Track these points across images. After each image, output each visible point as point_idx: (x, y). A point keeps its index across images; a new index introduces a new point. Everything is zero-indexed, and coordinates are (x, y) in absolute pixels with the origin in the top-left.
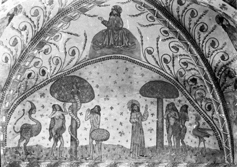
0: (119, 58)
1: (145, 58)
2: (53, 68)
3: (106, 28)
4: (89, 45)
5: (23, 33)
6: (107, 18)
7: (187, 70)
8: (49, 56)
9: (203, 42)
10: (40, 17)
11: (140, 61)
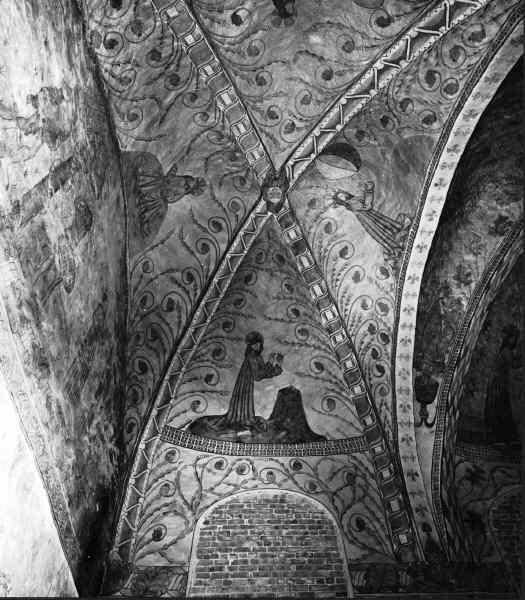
3: (165, 173)
7: (147, 345)
9: (211, 338)
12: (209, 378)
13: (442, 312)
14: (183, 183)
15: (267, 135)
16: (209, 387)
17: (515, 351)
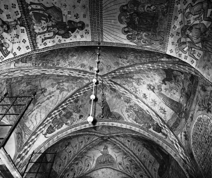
0: (107, 168)
1: (119, 167)
2: (79, 172)
3: (102, 154)
4: (95, 162)
5: (70, 154)
6: (102, 150)
8: (78, 166)
9: (141, 156)
10: (77, 148)
11: (116, 169)
12: (150, 162)
13: (137, 110)
14: (105, 150)
15: (93, 139)
16: (153, 163)
17: (156, 88)
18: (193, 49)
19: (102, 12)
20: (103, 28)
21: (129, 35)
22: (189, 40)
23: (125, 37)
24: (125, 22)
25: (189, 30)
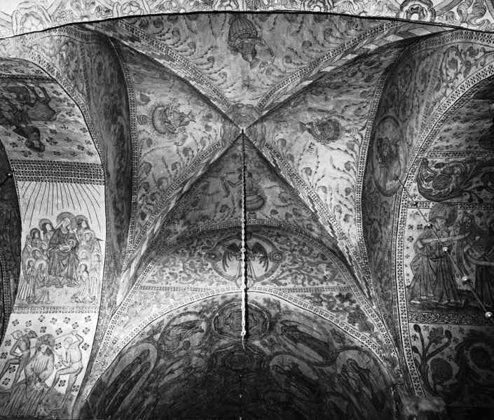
18: (17, 366)
19: (71, 182)
20: (44, 183)
21: (39, 233)
22: (33, 352)
23: (36, 225)
24: (62, 226)
25: (48, 348)
